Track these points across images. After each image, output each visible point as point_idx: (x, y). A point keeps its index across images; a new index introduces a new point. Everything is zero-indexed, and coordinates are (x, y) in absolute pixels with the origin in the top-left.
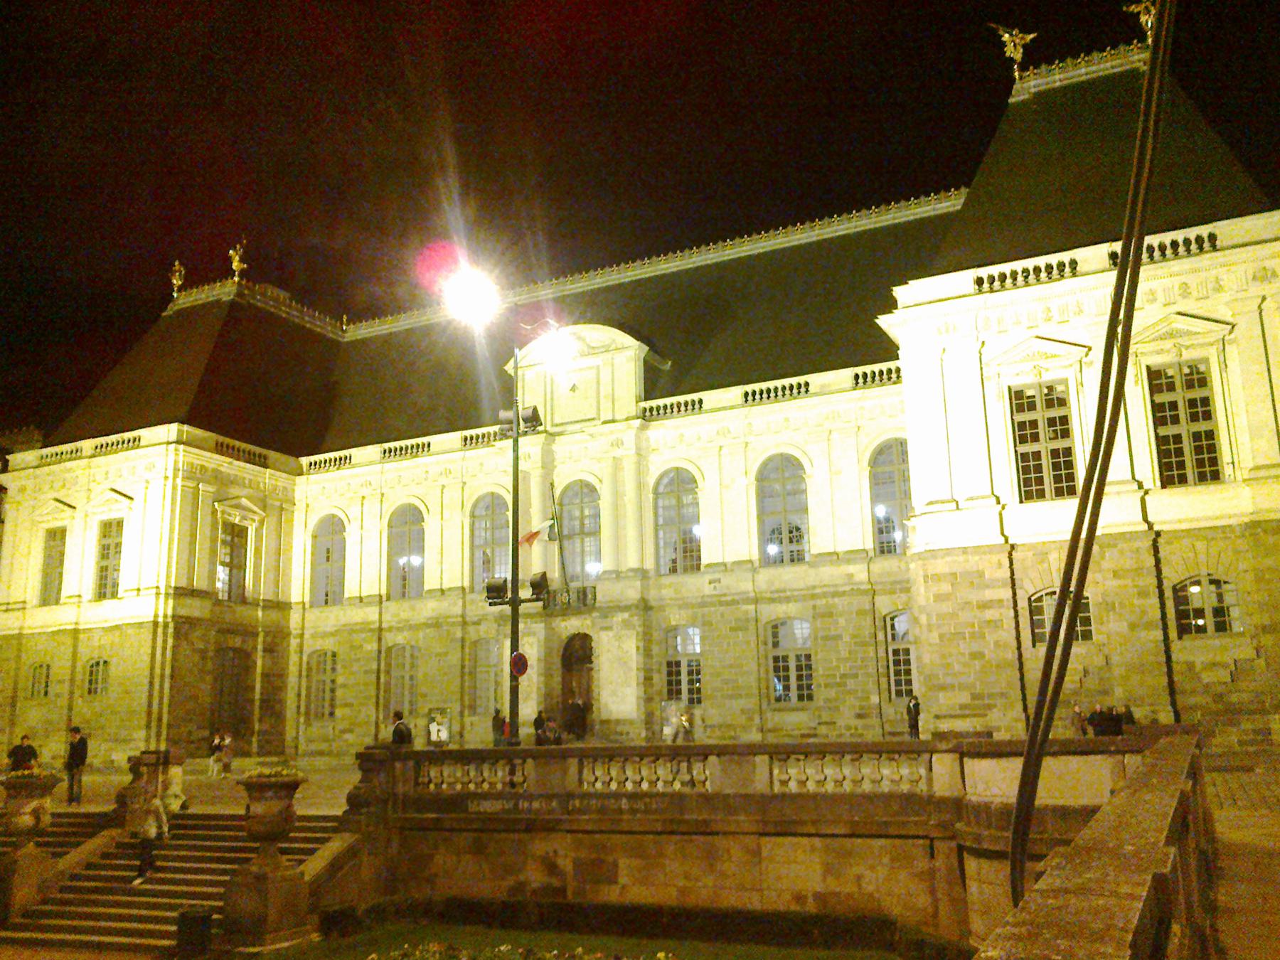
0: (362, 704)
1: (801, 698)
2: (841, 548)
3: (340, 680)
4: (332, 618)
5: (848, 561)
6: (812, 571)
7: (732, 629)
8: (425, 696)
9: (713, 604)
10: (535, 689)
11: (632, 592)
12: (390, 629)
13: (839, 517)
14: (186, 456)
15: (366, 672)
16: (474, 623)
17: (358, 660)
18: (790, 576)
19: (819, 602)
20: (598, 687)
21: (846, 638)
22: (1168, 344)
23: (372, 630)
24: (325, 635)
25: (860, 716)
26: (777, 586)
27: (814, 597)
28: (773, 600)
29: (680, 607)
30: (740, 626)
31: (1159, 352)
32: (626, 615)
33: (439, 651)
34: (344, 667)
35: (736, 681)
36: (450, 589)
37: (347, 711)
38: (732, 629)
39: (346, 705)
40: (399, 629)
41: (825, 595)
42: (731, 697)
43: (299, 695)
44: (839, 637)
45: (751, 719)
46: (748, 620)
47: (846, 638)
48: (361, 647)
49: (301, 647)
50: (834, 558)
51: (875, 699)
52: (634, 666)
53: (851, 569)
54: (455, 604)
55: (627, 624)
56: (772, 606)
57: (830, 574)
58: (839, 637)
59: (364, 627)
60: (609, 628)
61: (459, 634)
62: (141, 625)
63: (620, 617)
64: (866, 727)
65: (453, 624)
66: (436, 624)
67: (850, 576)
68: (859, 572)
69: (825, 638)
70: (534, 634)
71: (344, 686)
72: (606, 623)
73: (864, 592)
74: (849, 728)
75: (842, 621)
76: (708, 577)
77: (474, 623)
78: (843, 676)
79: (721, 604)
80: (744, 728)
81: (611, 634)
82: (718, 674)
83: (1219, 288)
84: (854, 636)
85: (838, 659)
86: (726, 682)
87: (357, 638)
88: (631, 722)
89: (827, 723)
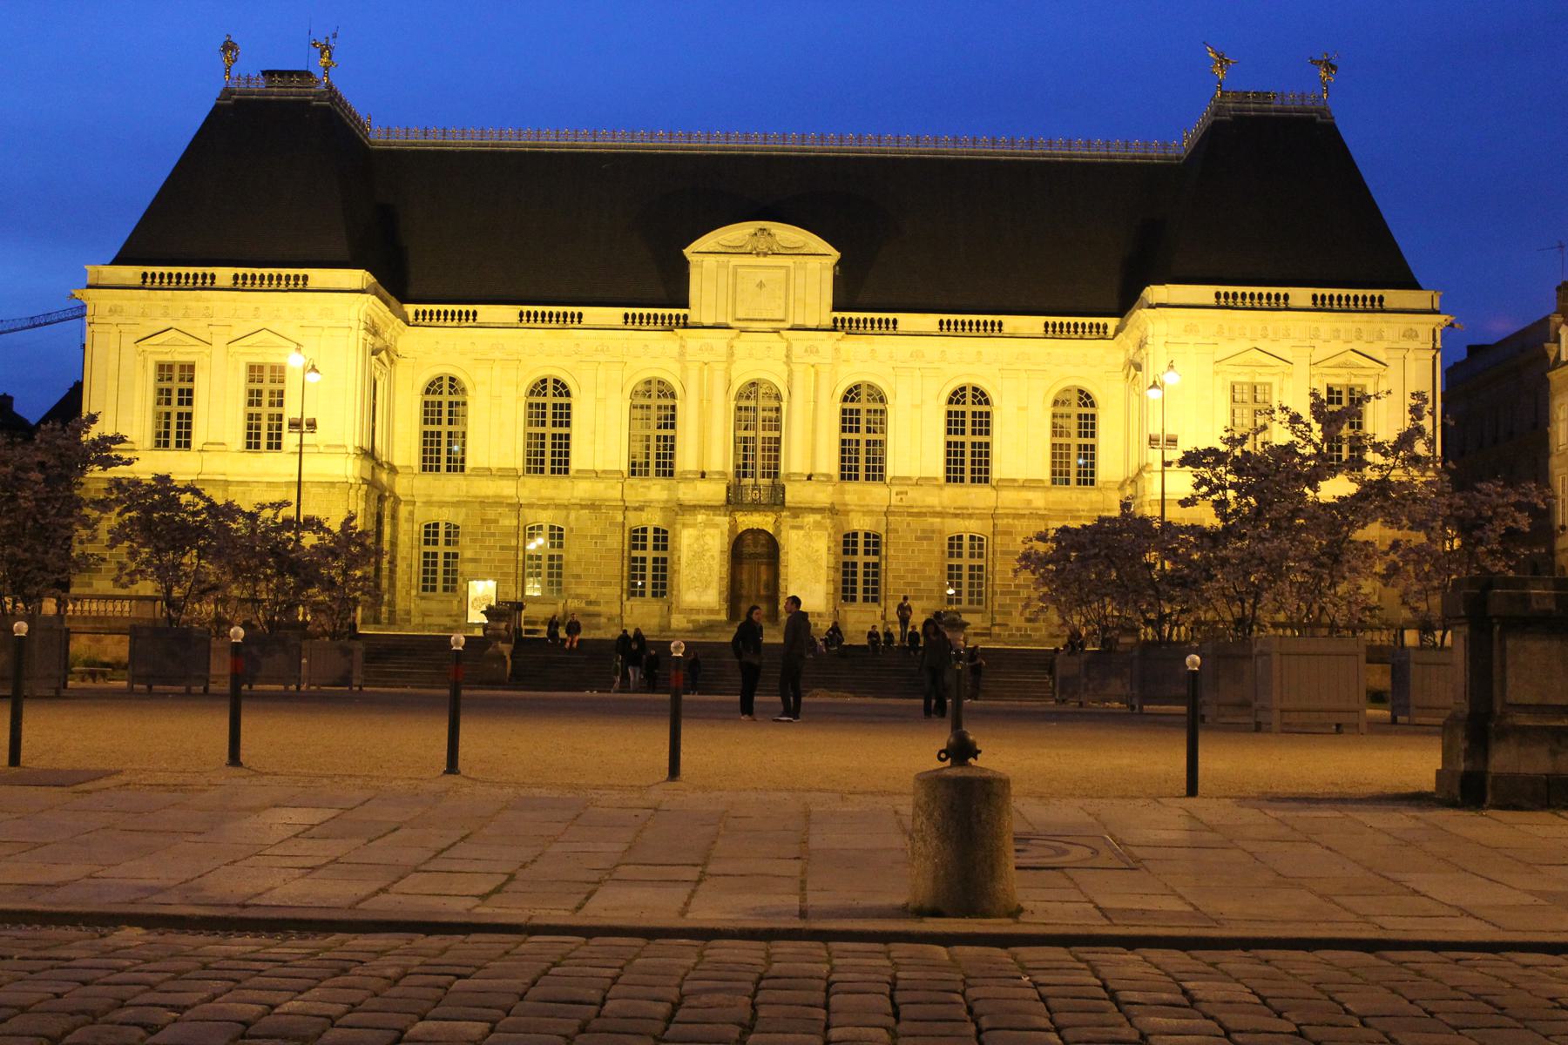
1: (971, 602)
2: (1021, 476)
3: (468, 554)
4: (447, 486)
7: (917, 538)
8: (578, 576)
9: (900, 514)
10: (716, 578)
11: (822, 495)
12: (531, 506)
14: (370, 305)
15: (502, 548)
16: (636, 509)
17: (493, 535)
18: (977, 496)
19: (999, 522)
22: (1344, 371)
23: (510, 505)
24: (442, 504)
26: (959, 504)
28: (956, 516)
29: (865, 513)
30: (926, 536)
31: (1337, 376)
32: (818, 517)
34: (474, 541)
35: (918, 584)
36: (604, 472)
38: (917, 538)
40: (545, 507)
41: (1007, 515)
43: (411, 566)
48: (496, 521)
49: (411, 513)
50: (1011, 483)
53: (1030, 495)
54: (613, 488)
55: (818, 525)
57: (1010, 498)
59: (498, 502)
60: (800, 528)
61: (620, 518)
62: (332, 484)
63: (811, 519)
64: (1033, 629)
66: (593, 506)
67: (1029, 502)
70: (717, 526)
72: (798, 522)
74: (1019, 629)
76: (895, 489)
77: (636, 509)
79: (910, 514)
81: (802, 533)
82: (902, 577)
83: (1381, 338)
86: (908, 584)
87: (491, 514)
88: (819, 615)
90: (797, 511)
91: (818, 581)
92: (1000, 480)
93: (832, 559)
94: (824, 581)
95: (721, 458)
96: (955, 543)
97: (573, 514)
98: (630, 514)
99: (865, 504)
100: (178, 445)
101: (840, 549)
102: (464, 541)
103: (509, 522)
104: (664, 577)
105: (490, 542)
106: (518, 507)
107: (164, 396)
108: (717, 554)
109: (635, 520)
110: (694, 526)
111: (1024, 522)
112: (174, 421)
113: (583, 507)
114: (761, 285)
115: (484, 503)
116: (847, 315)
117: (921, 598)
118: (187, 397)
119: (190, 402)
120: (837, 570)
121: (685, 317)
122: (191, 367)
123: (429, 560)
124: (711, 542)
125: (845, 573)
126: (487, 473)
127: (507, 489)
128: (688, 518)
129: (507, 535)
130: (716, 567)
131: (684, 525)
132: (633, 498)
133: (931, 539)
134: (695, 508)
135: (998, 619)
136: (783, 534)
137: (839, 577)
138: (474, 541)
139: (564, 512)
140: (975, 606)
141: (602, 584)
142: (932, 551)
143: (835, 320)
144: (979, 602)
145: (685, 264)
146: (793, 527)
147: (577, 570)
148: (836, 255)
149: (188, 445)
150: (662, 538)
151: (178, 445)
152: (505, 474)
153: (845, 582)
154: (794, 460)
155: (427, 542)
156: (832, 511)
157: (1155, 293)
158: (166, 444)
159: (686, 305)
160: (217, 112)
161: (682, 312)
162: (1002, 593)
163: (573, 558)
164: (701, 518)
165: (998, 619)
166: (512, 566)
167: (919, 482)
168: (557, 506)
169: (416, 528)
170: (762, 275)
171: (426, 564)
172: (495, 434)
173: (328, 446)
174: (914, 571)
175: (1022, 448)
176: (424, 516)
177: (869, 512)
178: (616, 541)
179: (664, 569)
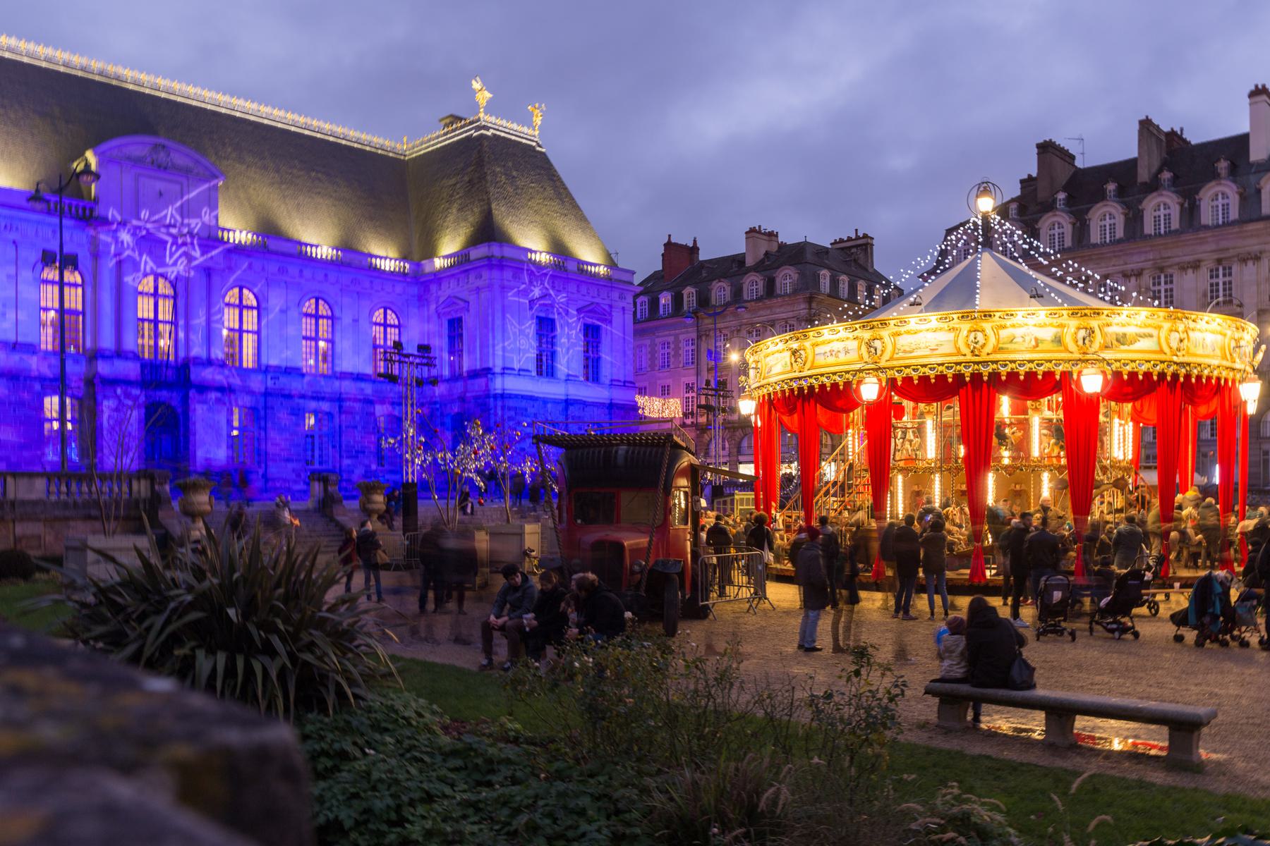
20: (194, 445)
28: (313, 398)
32: (219, 395)
51: (374, 467)
63: (213, 395)
75: (358, 418)
80: (296, 482)
81: (205, 407)
114: (161, 194)
136: (192, 407)
146: (199, 402)
162: (348, 457)
165: (345, 476)
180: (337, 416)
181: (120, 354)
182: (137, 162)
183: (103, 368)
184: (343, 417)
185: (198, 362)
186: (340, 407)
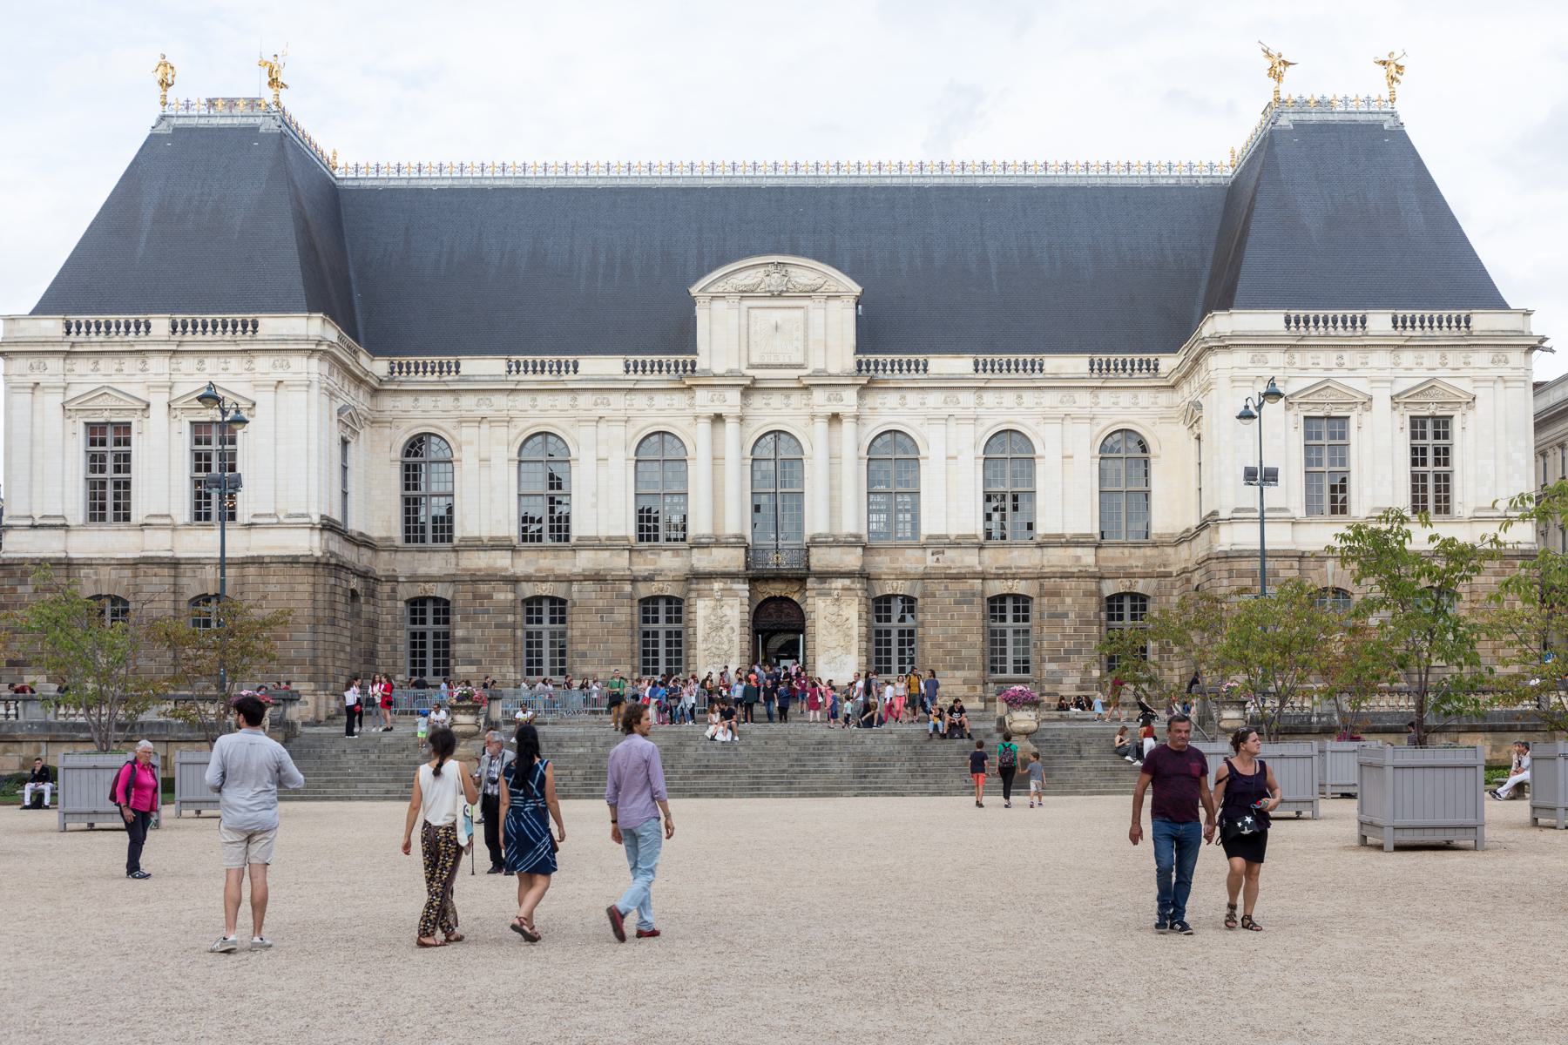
0: (492, 662)
1: (1016, 670)
3: (459, 633)
5: (1078, 544)
6: (1038, 551)
8: (584, 655)
10: (736, 652)
11: (851, 559)
13: (1066, 500)
15: (498, 626)
19: (1048, 583)
21: (1072, 615)
24: (429, 579)
25: (1080, 688)
27: (1040, 577)
28: (998, 577)
30: (965, 599)
32: (847, 582)
33: (600, 603)
37: (473, 669)
39: (471, 663)
40: (544, 580)
41: (1053, 576)
42: (955, 668)
44: (1065, 615)
45: (974, 689)
46: (974, 595)
47: (1072, 615)
48: (490, 597)
51: (1096, 673)
52: (855, 632)
53: (1079, 551)
56: (997, 582)
57: (1057, 558)
58: (1065, 615)
59: (492, 577)
63: (839, 583)
65: (622, 579)
66: (598, 578)
67: (1078, 558)
68: (1087, 557)
69: (1053, 616)
71: (466, 640)
73: (1092, 576)
75: (1068, 600)
78: (1067, 652)
81: (829, 600)
82: (940, 646)
84: (1079, 616)
85: (1063, 635)
86: (949, 653)
89: (1049, 694)
90: (824, 576)
91: (849, 652)
92: (1047, 536)
93: (864, 630)
94: (855, 650)
95: (736, 521)
96: (996, 605)
97: (575, 587)
98: (640, 585)
99: (899, 568)
100: (117, 518)
101: (872, 616)
102: (456, 618)
103: (504, 596)
104: (679, 653)
105: (483, 619)
106: (514, 581)
107: (96, 462)
108: (737, 626)
109: (645, 590)
110: (709, 594)
111: (1073, 583)
112: (110, 491)
113: (586, 578)
115: (475, 579)
116: (872, 358)
117: (963, 668)
118: (124, 462)
119: (128, 470)
120: (868, 641)
121: (693, 364)
122: (127, 427)
123: (417, 641)
124: (727, 611)
125: (878, 643)
126: (477, 545)
127: (501, 561)
128: (702, 586)
129: (503, 612)
130: (736, 638)
131: (699, 596)
132: (642, 566)
133: (971, 603)
134: (710, 576)
135: (1048, 688)
136: (810, 601)
137: (873, 646)
138: (465, 619)
139: (565, 585)
140: (1022, 676)
141: (611, 663)
142: (972, 617)
143: (859, 363)
144: (1026, 670)
145: (692, 302)
147: (581, 647)
148: (857, 289)
149: (127, 518)
150: (676, 607)
151: (117, 518)
152: (497, 545)
153: (878, 652)
154: (815, 522)
155: (414, 621)
156: (864, 576)
157: (1219, 323)
158: (103, 518)
159: (694, 351)
160: (153, 141)
161: (689, 358)
162: (1052, 660)
163: (576, 633)
164: (717, 585)
165: (1048, 688)
166: (509, 646)
167: (958, 543)
168: (558, 579)
169: (401, 604)
170: (777, 316)
171: (414, 645)
172: (486, 500)
173: (289, 516)
174: (954, 639)
175: (1066, 500)
176: (406, 592)
177: (904, 576)
178: (625, 614)
179: (679, 644)
180: (1036, 601)
181: (717, 542)
182: (745, 294)
183: (703, 561)
184: (1045, 600)
185: (815, 542)
186: (1041, 585)
